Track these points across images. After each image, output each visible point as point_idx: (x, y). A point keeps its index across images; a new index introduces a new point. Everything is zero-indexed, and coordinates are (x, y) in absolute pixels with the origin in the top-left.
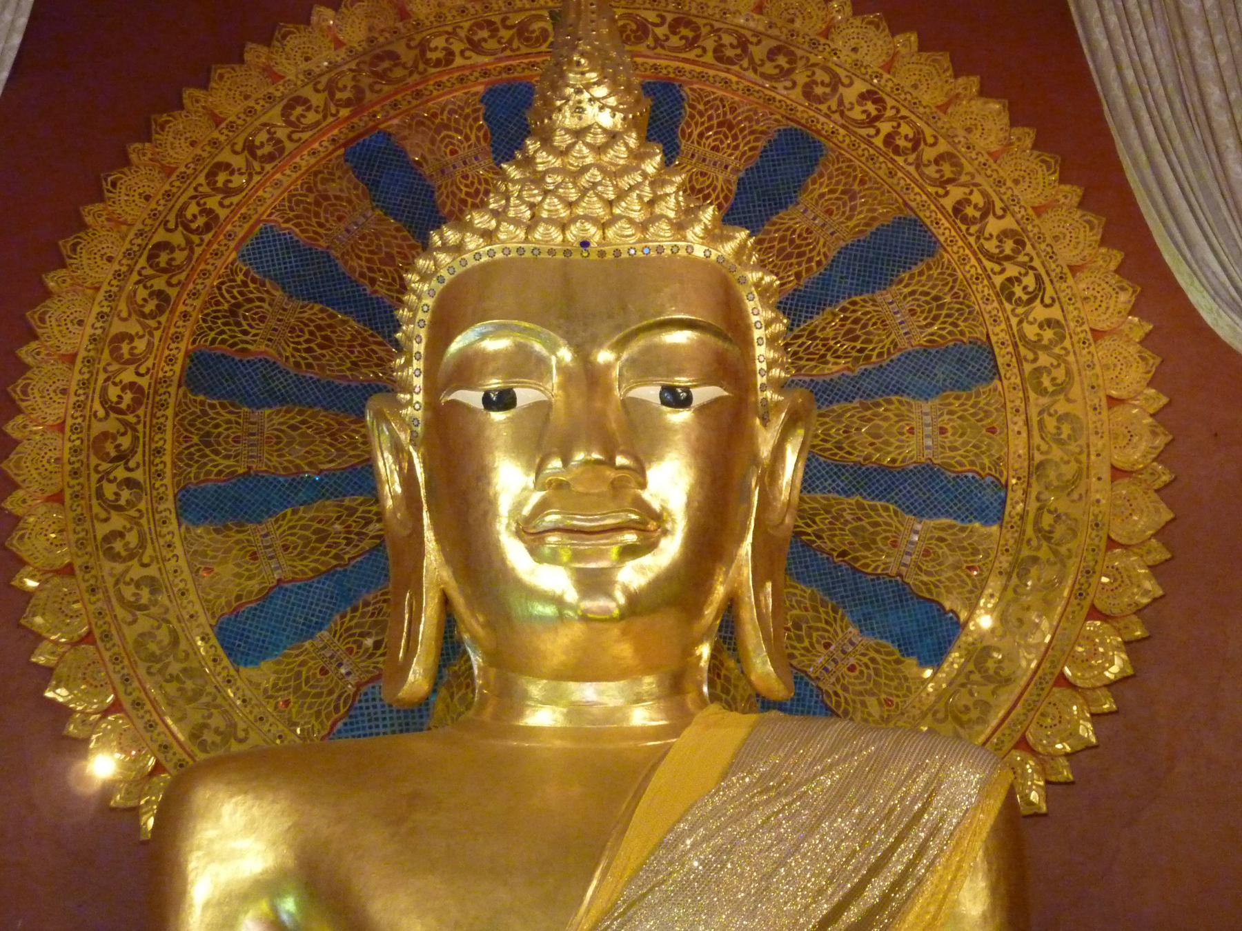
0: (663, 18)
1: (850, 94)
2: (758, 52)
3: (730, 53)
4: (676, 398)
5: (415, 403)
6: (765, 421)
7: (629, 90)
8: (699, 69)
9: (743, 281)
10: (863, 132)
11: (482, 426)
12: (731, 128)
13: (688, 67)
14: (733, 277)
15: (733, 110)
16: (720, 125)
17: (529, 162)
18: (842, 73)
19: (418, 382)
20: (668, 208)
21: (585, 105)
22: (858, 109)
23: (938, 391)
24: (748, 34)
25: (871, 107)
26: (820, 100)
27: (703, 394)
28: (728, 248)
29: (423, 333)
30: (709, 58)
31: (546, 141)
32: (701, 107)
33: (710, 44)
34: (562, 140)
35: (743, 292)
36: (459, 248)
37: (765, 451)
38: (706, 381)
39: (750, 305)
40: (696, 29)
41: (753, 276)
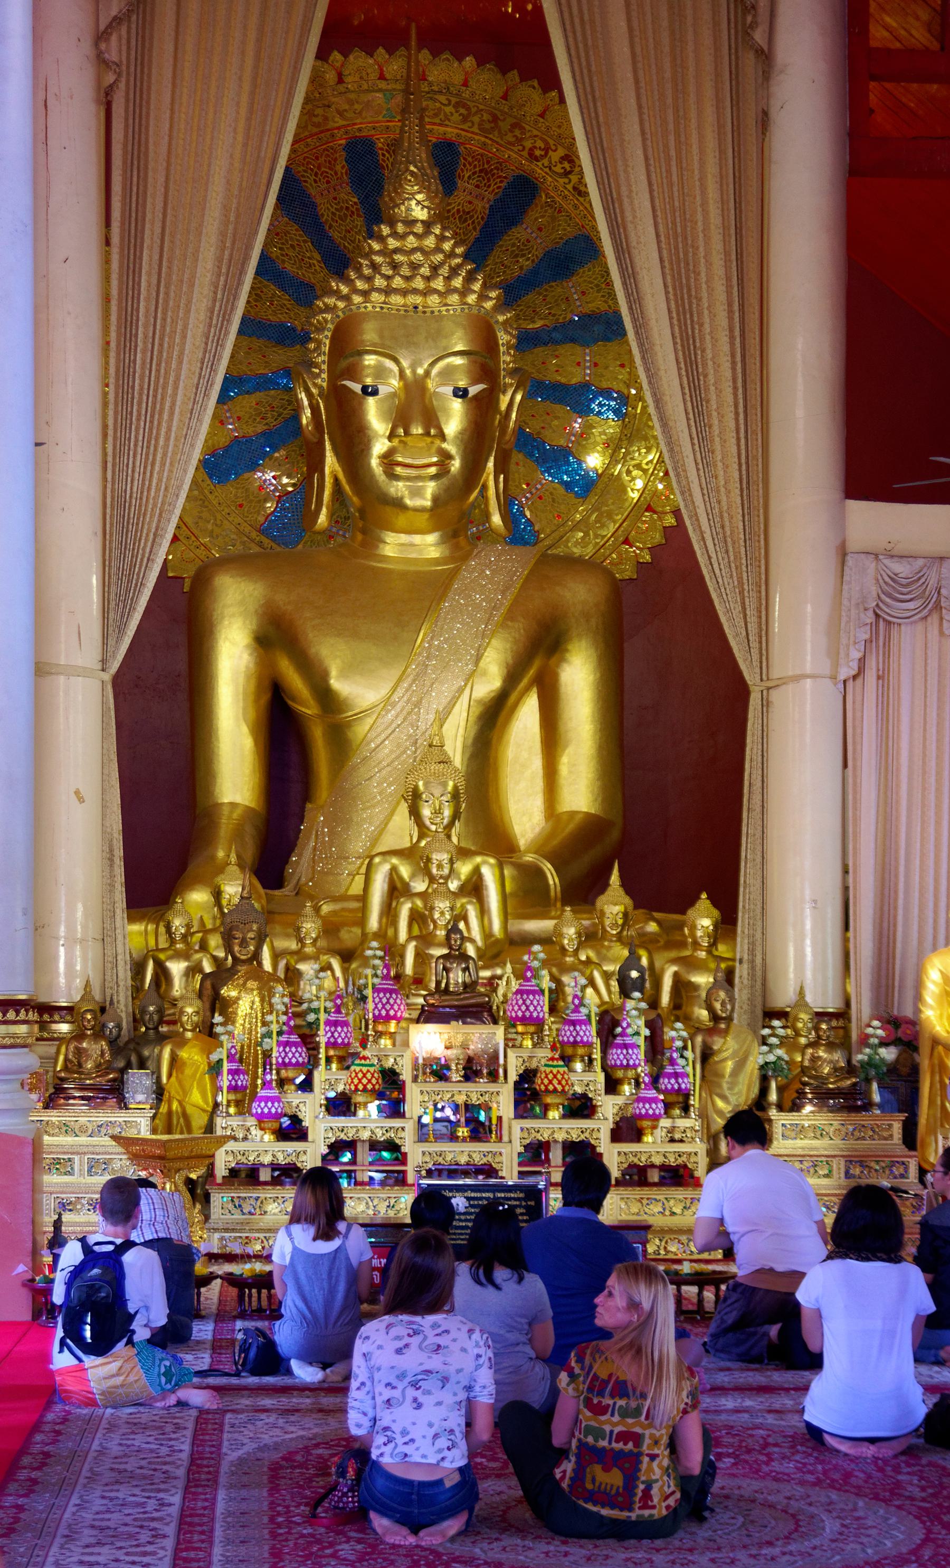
0: (450, 101)
1: (555, 156)
2: (504, 126)
3: (488, 126)
4: (461, 393)
5: (323, 380)
6: (504, 392)
7: (436, 196)
8: (470, 135)
9: (497, 322)
10: (562, 181)
11: (361, 404)
12: (486, 174)
13: (463, 133)
14: (492, 321)
15: (488, 162)
16: (481, 171)
17: (382, 239)
18: (551, 142)
19: (325, 367)
20: (458, 282)
21: (414, 207)
22: (559, 166)
23: (596, 341)
24: (499, 114)
25: (567, 165)
26: (537, 159)
27: (473, 390)
28: (489, 305)
29: (327, 342)
30: (475, 129)
31: (392, 224)
32: (470, 159)
33: (476, 119)
34: (400, 228)
35: (496, 327)
36: (347, 298)
37: (503, 406)
38: (475, 382)
39: (499, 334)
40: (468, 109)
41: (501, 318)
